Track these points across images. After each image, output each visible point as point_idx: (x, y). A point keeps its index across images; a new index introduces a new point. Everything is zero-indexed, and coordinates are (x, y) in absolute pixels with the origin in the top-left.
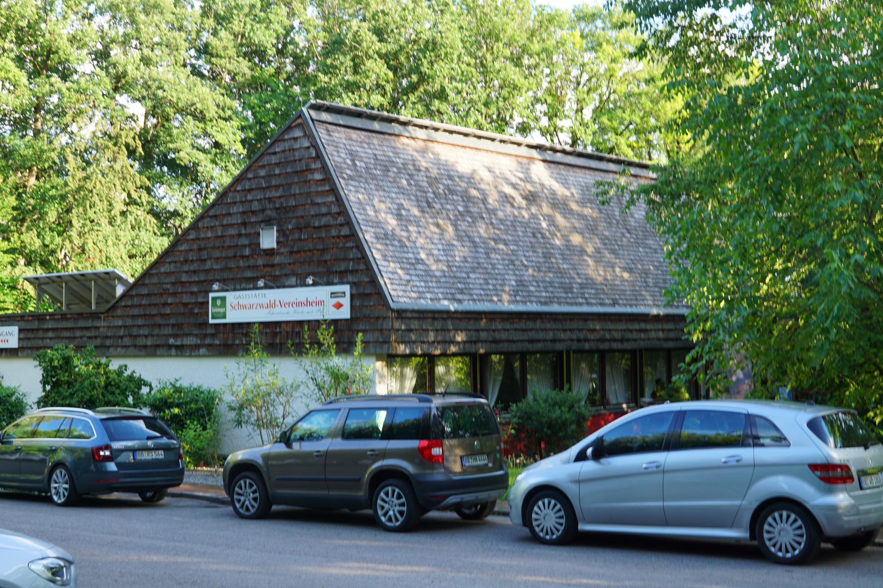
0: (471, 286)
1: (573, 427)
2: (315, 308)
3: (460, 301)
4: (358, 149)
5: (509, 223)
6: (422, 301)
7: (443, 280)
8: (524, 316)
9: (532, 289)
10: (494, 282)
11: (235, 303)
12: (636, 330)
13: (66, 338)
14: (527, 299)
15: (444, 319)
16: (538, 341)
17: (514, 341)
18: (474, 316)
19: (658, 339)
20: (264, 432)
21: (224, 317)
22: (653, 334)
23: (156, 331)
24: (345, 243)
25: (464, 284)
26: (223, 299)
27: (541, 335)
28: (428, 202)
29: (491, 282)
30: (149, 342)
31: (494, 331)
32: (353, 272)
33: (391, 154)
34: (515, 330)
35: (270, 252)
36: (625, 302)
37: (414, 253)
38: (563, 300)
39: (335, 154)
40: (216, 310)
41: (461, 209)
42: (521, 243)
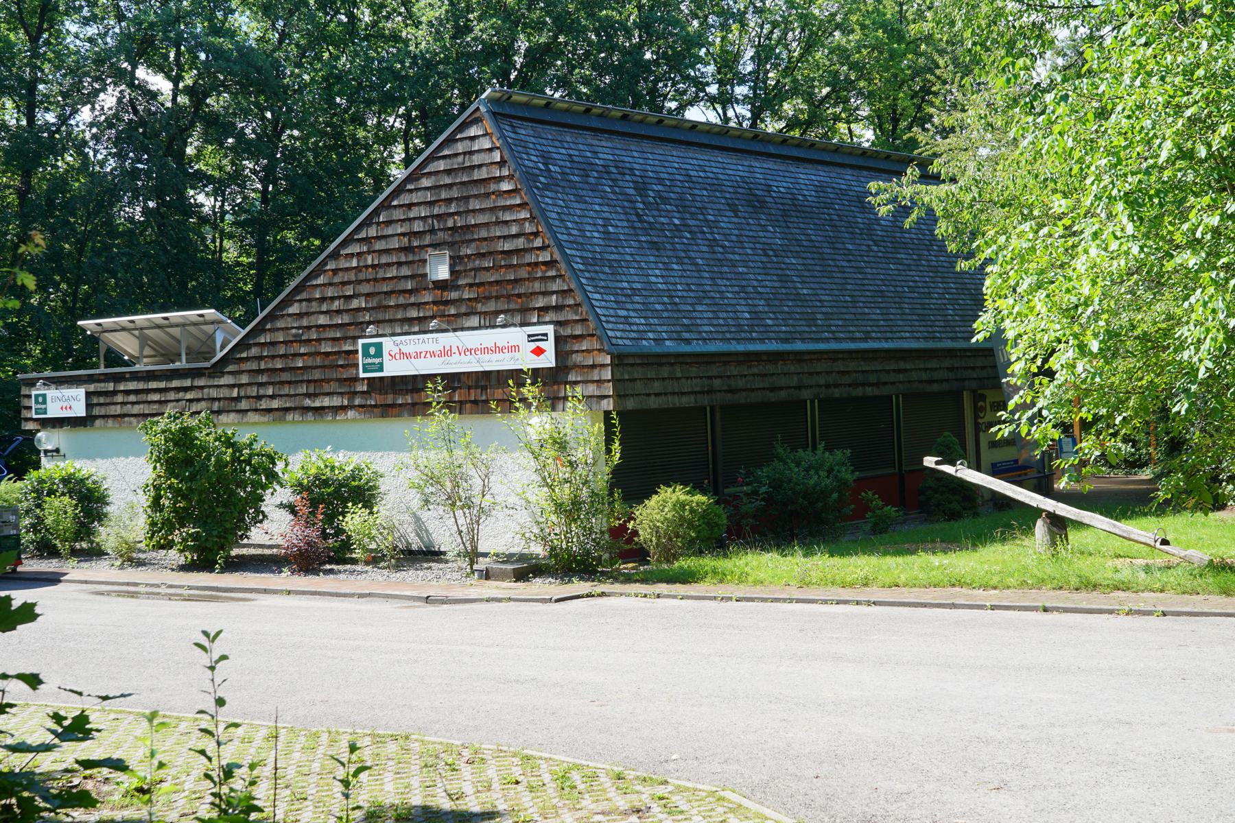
0: (698, 321)
1: (835, 495)
2: (507, 355)
3: (688, 341)
4: (551, 149)
5: (734, 238)
6: (644, 342)
7: (665, 314)
8: (765, 358)
9: (769, 322)
10: (725, 315)
11: (395, 350)
12: (894, 371)
13: (155, 402)
14: (765, 336)
15: (672, 364)
16: (781, 388)
17: (752, 390)
18: (705, 359)
19: (921, 382)
20: (459, 513)
21: (381, 369)
22: (915, 376)
23: (286, 390)
24: (546, 271)
25: (691, 318)
26: (379, 347)
27: (783, 381)
28: (638, 215)
29: (721, 315)
30: (275, 404)
31: (729, 377)
32: (558, 308)
33: (589, 154)
34: (753, 375)
35: (441, 285)
36: (879, 335)
37: (628, 282)
38: (806, 336)
39: (524, 156)
40: (369, 361)
41: (677, 222)
42: (750, 264)
